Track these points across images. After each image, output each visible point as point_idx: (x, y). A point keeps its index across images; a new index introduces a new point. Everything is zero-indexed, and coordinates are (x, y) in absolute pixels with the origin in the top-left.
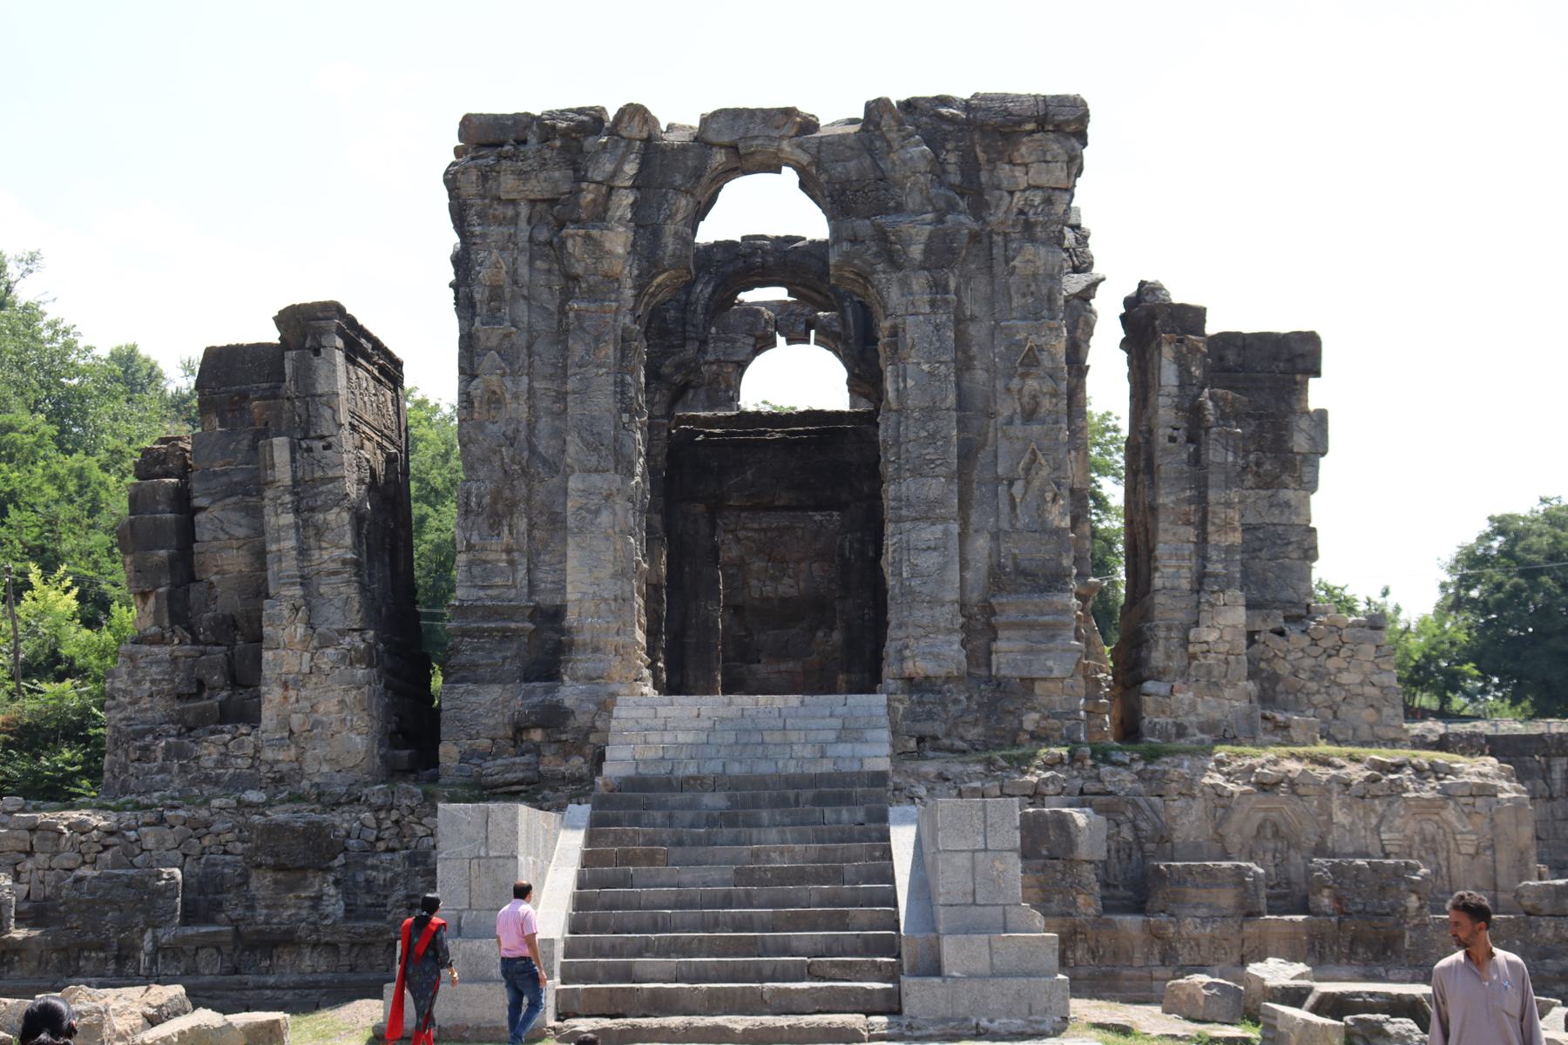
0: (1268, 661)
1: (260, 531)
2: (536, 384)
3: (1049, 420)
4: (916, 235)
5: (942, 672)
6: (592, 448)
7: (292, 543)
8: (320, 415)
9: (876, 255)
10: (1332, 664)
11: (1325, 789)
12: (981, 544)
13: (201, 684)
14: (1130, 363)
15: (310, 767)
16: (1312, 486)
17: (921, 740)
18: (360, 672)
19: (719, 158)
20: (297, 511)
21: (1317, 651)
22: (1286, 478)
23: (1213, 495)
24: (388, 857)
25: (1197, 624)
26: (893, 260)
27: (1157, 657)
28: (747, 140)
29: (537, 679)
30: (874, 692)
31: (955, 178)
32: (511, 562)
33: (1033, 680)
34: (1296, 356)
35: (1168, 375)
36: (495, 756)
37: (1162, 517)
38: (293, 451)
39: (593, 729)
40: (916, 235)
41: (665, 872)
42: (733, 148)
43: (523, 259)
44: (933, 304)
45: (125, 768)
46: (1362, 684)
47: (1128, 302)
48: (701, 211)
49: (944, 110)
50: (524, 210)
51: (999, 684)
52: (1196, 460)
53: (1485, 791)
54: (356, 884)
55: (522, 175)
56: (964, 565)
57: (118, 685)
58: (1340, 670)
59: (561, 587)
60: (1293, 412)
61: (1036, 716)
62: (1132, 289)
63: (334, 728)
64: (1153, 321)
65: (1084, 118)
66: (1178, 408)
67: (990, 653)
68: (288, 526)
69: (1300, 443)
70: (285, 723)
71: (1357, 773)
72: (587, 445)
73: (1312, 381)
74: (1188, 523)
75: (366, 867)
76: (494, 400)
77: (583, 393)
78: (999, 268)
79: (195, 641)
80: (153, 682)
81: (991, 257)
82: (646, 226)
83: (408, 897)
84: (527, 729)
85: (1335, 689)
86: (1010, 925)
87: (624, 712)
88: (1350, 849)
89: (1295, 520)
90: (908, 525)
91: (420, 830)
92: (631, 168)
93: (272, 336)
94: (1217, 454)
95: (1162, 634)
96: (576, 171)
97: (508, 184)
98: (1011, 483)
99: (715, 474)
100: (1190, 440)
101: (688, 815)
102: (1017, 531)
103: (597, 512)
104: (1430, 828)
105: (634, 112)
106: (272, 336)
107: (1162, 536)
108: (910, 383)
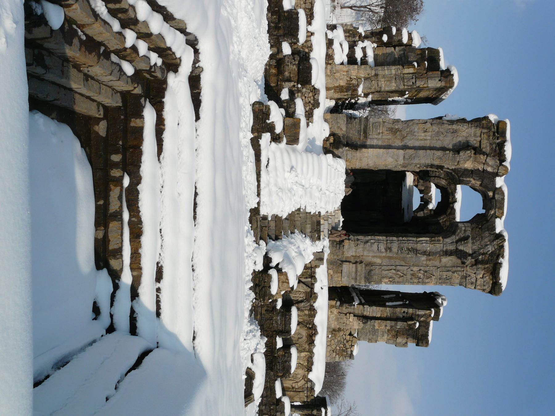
2: (428, 141)
8: (422, 81)
14: (420, 293)
20: (396, 75)
21: (345, 342)
32: (379, 133)
42: (494, 197)
56: (373, 257)
60: (407, 338)
61: (332, 273)
66: (412, 314)
72: (411, 156)
73: (415, 344)
78: (454, 269)
89: (379, 338)
92: (489, 169)
100: (403, 316)
103: (392, 158)
104: (299, 376)
108: (424, 244)
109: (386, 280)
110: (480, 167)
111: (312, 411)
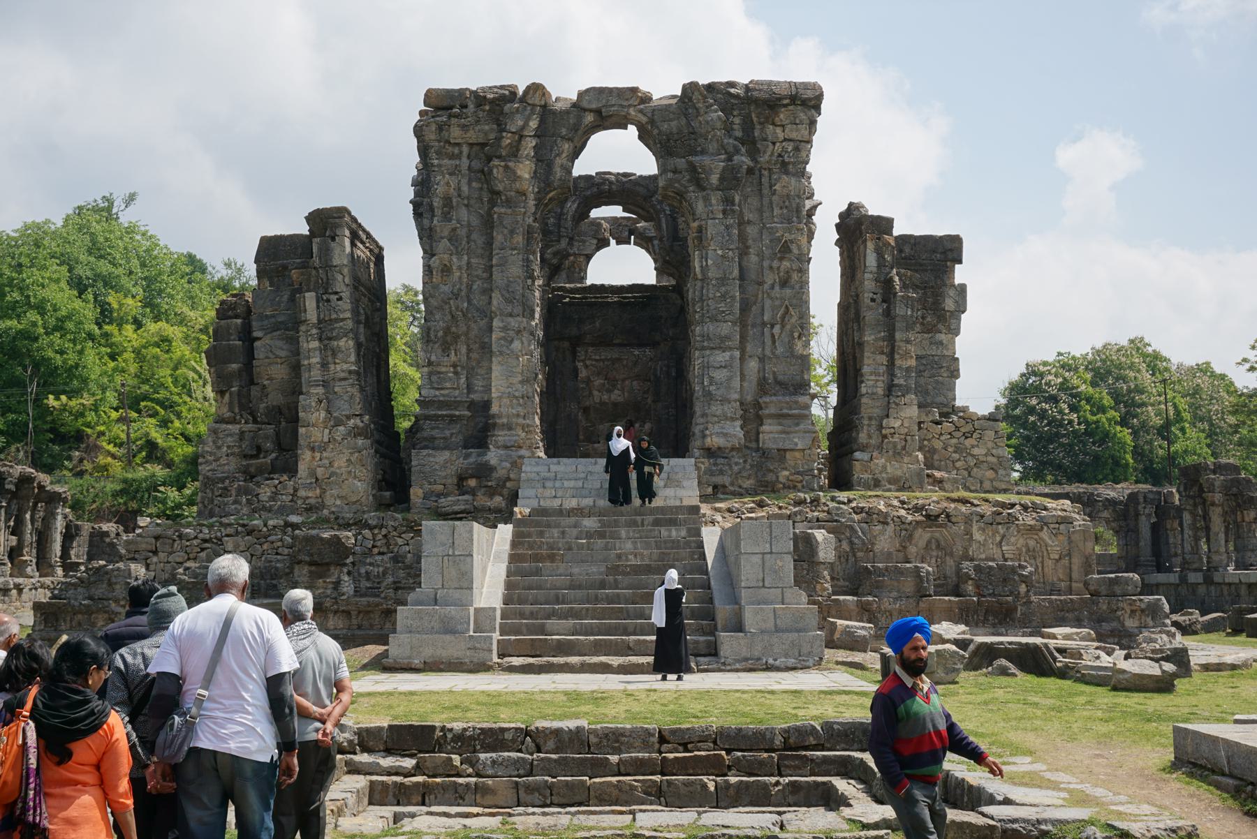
0: (929, 440)
1: (297, 353)
3: (797, 287)
4: (714, 166)
5: (729, 445)
6: (509, 301)
7: (318, 360)
8: (335, 279)
9: (689, 181)
10: (968, 442)
11: (968, 520)
12: (753, 365)
13: (259, 449)
14: (841, 254)
15: (329, 501)
16: (957, 333)
17: (715, 487)
18: (360, 442)
19: (589, 118)
20: (320, 340)
21: (957, 434)
22: (940, 326)
23: (898, 335)
24: (380, 558)
25: (887, 416)
26: (700, 186)
27: (863, 437)
28: (606, 108)
29: (472, 447)
30: (684, 457)
31: (739, 134)
32: (456, 373)
33: (785, 450)
34: (945, 252)
35: (871, 260)
36: (446, 495)
37: (866, 349)
38: (318, 302)
39: (509, 479)
40: (714, 166)
41: (562, 567)
42: (598, 112)
43: (464, 181)
44: (724, 212)
45: (212, 501)
46: (986, 455)
47: (841, 216)
48: (576, 153)
49: (732, 90)
50: (465, 149)
51: (764, 453)
52: (888, 313)
53: (1067, 521)
54: (360, 574)
55: (464, 128)
57: (207, 449)
58: (973, 447)
59: (488, 389)
60: (945, 285)
61: (786, 473)
62: (844, 207)
63: (344, 477)
64: (857, 228)
65: (820, 97)
67: (758, 433)
68: (315, 349)
69: (949, 304)
70: (313, 473)
71: (987, 510)
72: (506, 300)
74: (882, 353)
75: (365, 564)
76: (446, 270)
77: (503, 264)
78: (766, 191)
79: (255, 421)
80: (228, 447)
81: (760, 183)
82: (543, 160)
83: (395, 583)
84: (466, 478)
85: (970, 458)
86: (786, 601)
87: (529, 468)
88: (983, 556)
89: (945, 352)
90: (708, 352)
91: (400, 541)
92: (533, 124)
93: (304, 229)
94: (900, 310)
95: (866, 422)
96: (499, 125)
97: (455, 133)
98: (772, 326)
99: (581, 323)
100: (884, 301)
101: (575, 532)
102: (777, 357)
103: (512, 341)
104: (1032, 543)
105: (536, 89)
106: (304, 229)
107: (866, 361)
108: (710, 262)
109: (799, 346)
110: (530, 144)
111: (1213, 504)
